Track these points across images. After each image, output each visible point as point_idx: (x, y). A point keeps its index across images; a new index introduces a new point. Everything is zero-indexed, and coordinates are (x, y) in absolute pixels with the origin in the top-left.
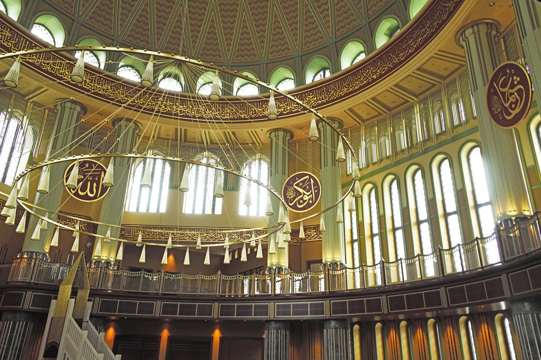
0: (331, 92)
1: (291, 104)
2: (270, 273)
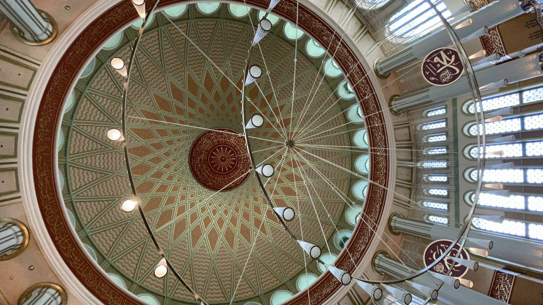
0: (67, 69)
1: (98, 31)
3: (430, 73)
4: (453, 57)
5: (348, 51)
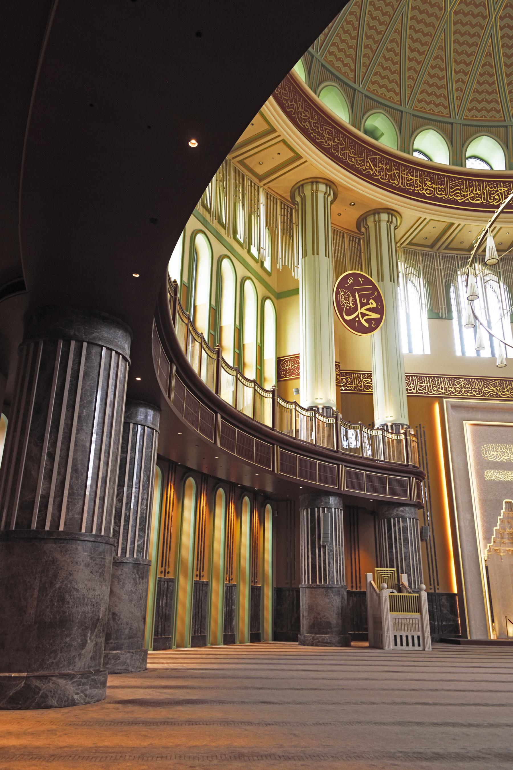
3: (359, 284)
4: (367, 325)
5: (455, 202)
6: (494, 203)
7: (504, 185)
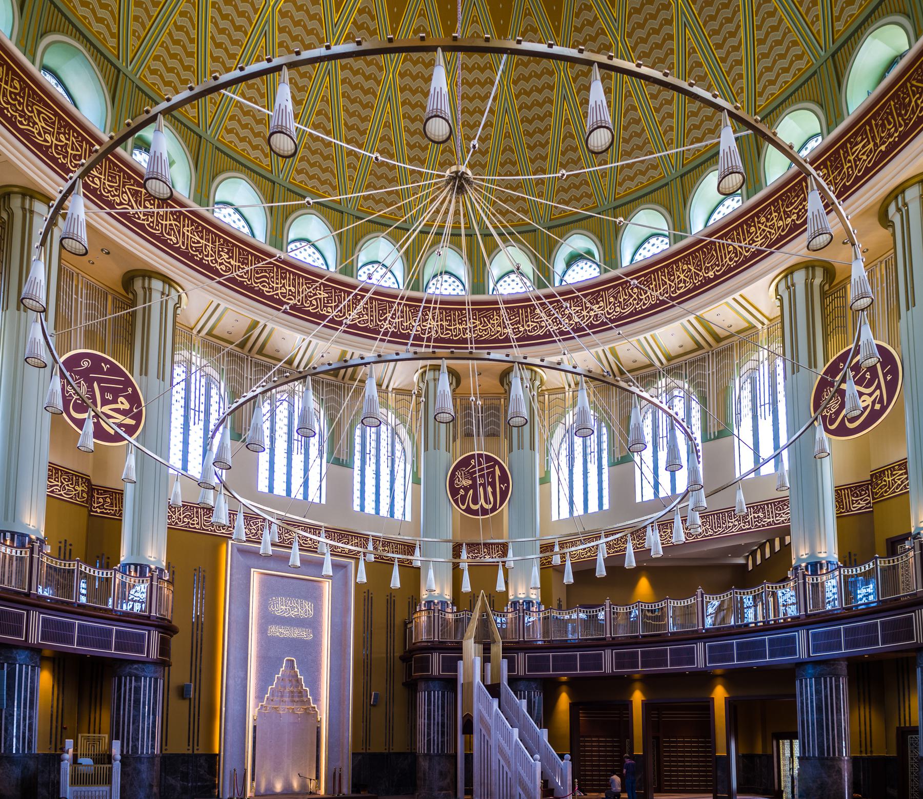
2: (796, 576)
6: (310, 308)
7: (324, 290)
